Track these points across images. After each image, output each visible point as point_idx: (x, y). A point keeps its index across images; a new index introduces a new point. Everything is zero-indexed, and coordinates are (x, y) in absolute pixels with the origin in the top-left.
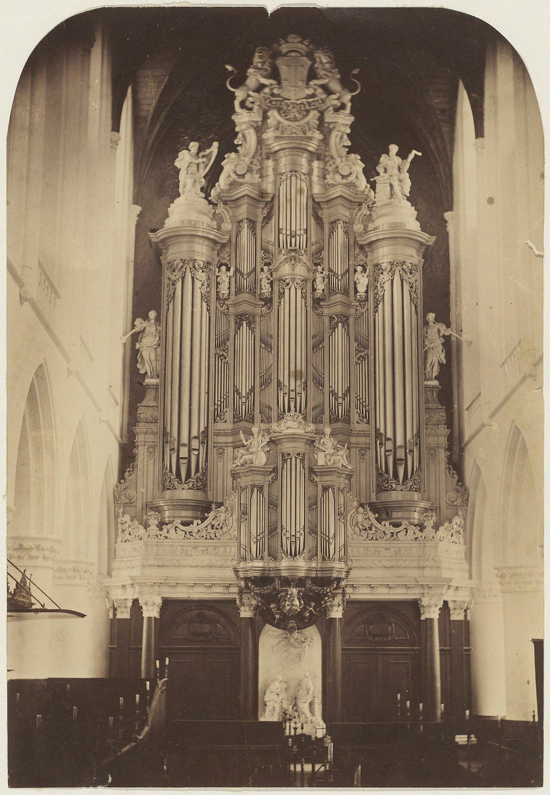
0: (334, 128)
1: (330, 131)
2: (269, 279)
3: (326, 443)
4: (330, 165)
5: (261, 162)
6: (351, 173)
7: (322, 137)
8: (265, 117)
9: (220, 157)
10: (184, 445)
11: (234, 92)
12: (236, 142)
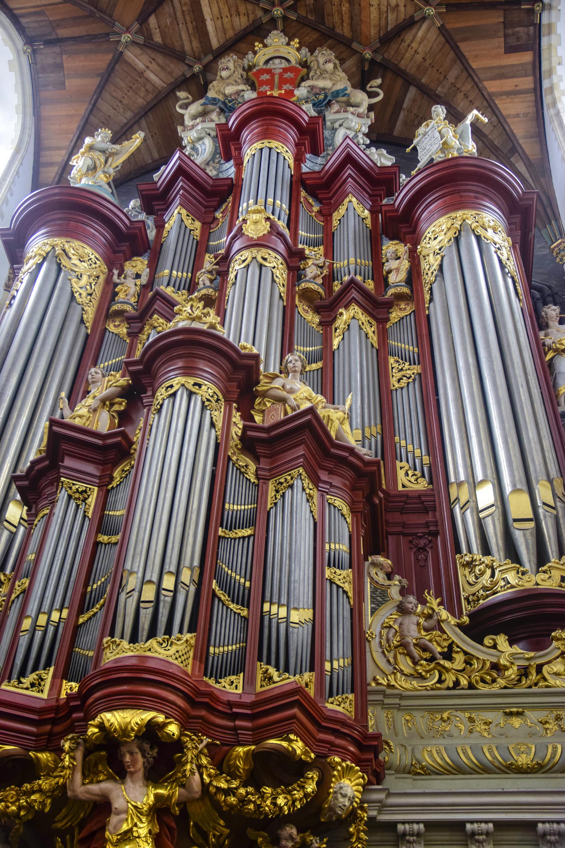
0: (340, 125)
3: (288, 387)
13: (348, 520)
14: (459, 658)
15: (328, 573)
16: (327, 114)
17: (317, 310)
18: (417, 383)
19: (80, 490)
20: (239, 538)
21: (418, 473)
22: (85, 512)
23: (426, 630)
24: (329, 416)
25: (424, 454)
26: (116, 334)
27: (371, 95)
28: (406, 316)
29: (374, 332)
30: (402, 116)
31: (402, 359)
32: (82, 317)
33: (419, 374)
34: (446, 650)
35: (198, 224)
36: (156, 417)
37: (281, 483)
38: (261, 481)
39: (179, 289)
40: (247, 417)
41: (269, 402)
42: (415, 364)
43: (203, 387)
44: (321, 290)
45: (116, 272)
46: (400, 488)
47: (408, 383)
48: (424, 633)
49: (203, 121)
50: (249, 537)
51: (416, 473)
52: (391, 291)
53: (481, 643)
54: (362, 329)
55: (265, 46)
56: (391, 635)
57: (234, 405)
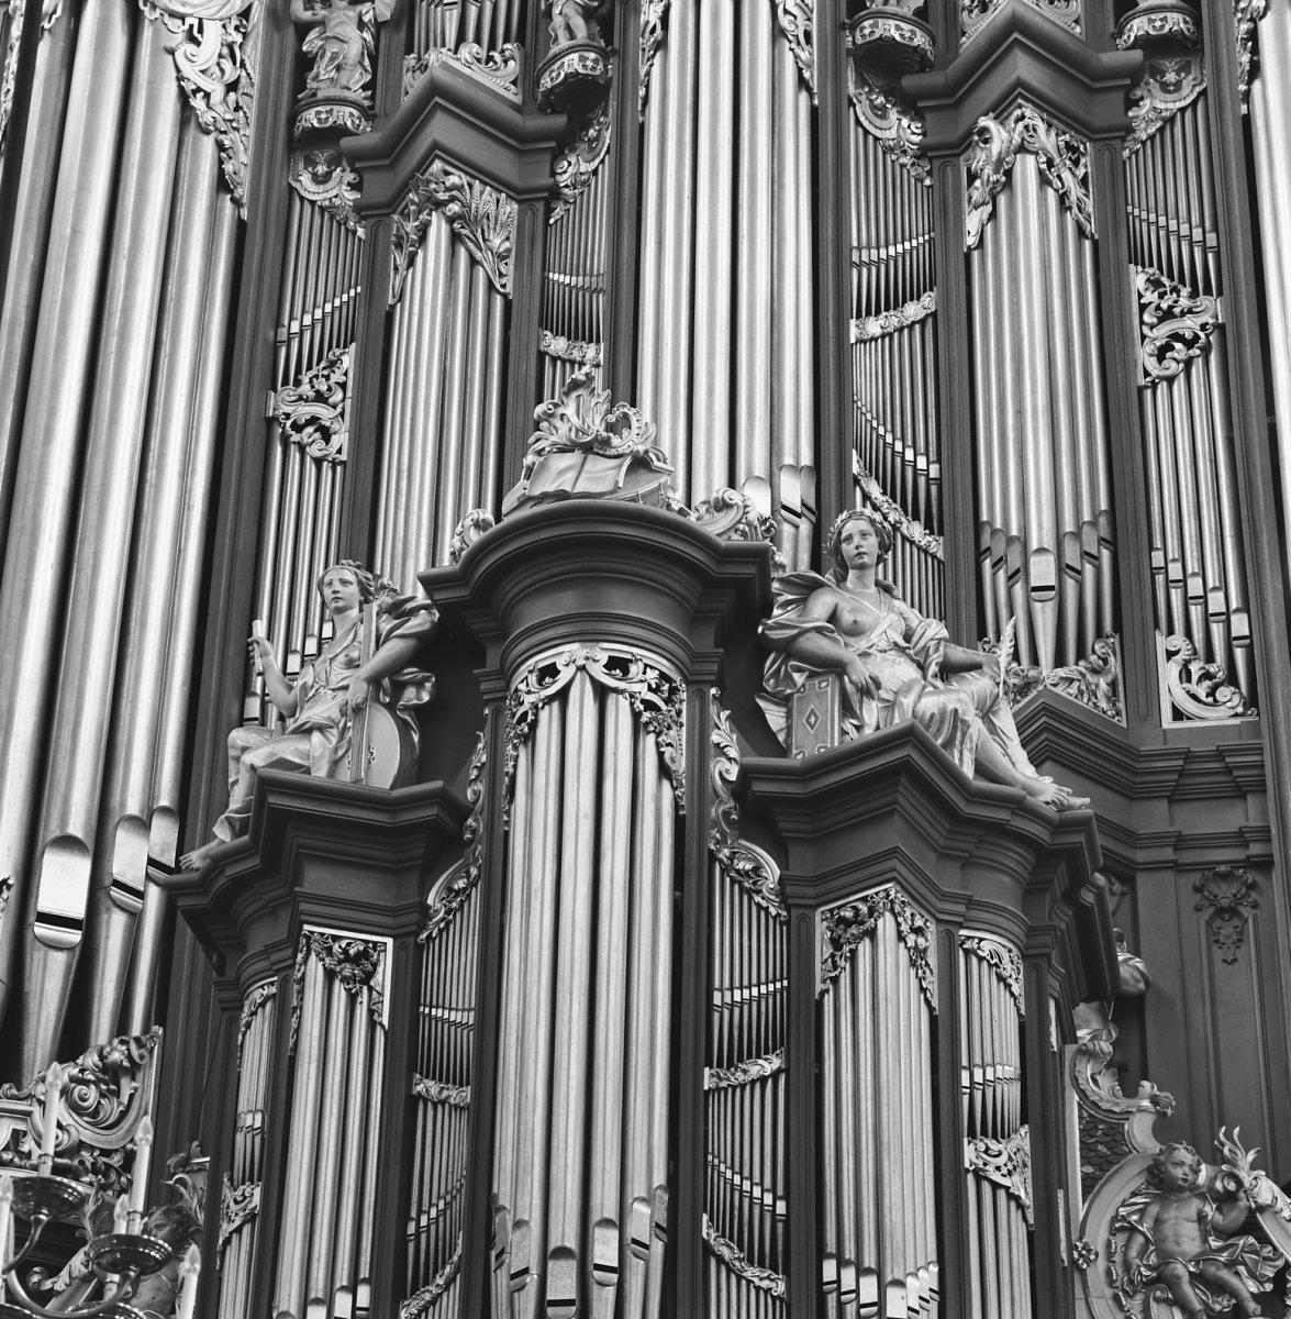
3: (847, 618)
13: (1016, 989)
15: (970, 1154)
17: (910, 106)
18: (1213, 358)
19: (352, 952)
20: (753, 1082)
21: (1218, 667)
22: (371, 1012)
23: (1221, 1233)
24: (956, 711)
25: (1234, 605)
26: (322, 209)
28: (1183, 110)
29: (1084, 182)
31: (1171, 277)
32: (221, 172)
33: (1220, 328)
34: (1269, 1287)
36: (523, 753)
37: (847, 923)
38: (794, 912)
39: (492, 46)
40: (751, 726)
41: (799, 670)
42: (1208, 291)
43: (633, 669)
44: (920, 40)
46: (1167, 721)
47: (1188, 363)
48: (1214, 1243)
50: (775, 1075)
51: (1212, 669)
54: (1050, 184)
56: (1133, 1253)
57: (713, 691)
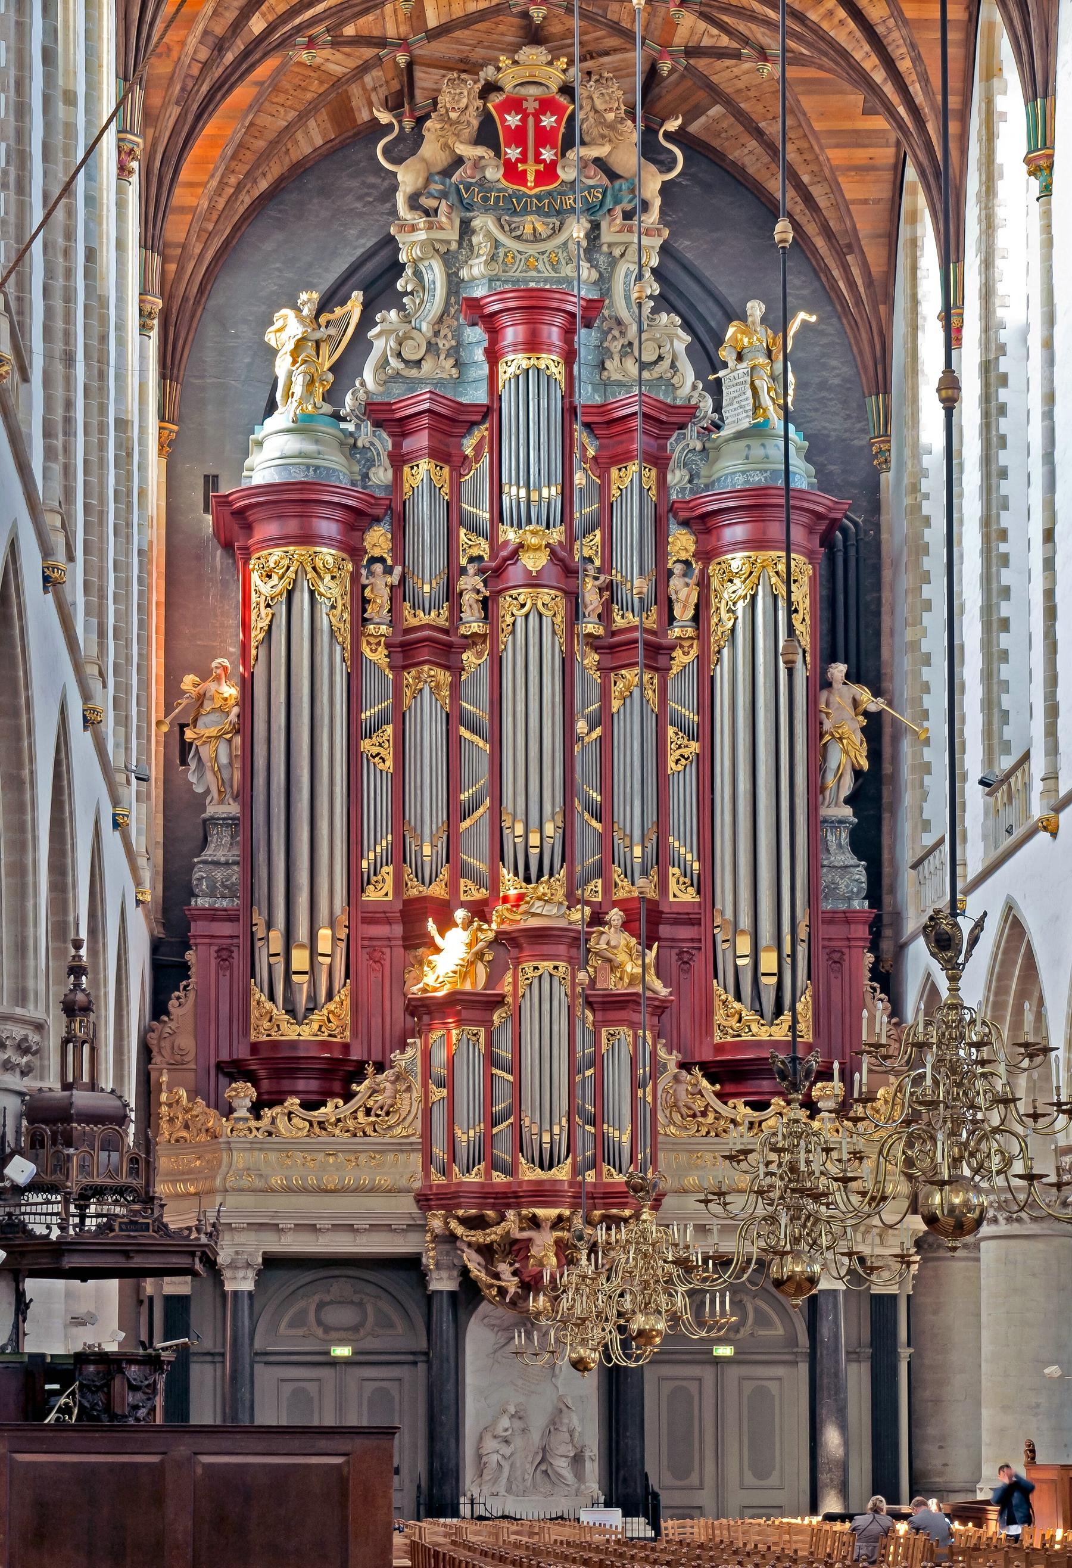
0: (623, 255)
1: (613, 262)
2: (478, 592)
4: (614, 338)
5: (457, 335)
6: (660, 358)
7: (595, 275)
8: (466, 229)
9: (366, 321)
10: (302, 946)
11: (395, 174)
12: (400, 285)
14: (711, 1116)
16: (604, 225)
27: (666, 165)
30: (703, 119)
35: (446, 470)
45: (364, 572)
49: (430, 228)
52: (677, 632)
53: (726, 1103)
55: (516, 63)
